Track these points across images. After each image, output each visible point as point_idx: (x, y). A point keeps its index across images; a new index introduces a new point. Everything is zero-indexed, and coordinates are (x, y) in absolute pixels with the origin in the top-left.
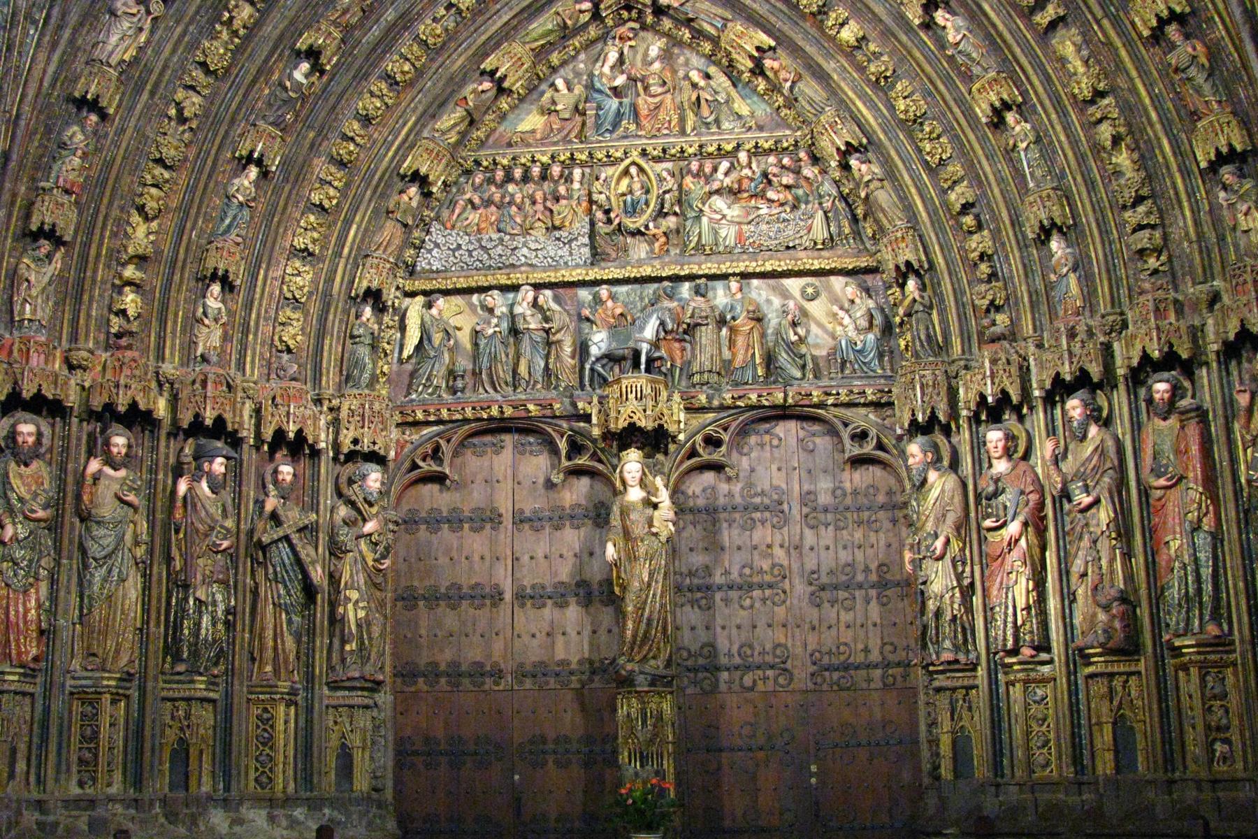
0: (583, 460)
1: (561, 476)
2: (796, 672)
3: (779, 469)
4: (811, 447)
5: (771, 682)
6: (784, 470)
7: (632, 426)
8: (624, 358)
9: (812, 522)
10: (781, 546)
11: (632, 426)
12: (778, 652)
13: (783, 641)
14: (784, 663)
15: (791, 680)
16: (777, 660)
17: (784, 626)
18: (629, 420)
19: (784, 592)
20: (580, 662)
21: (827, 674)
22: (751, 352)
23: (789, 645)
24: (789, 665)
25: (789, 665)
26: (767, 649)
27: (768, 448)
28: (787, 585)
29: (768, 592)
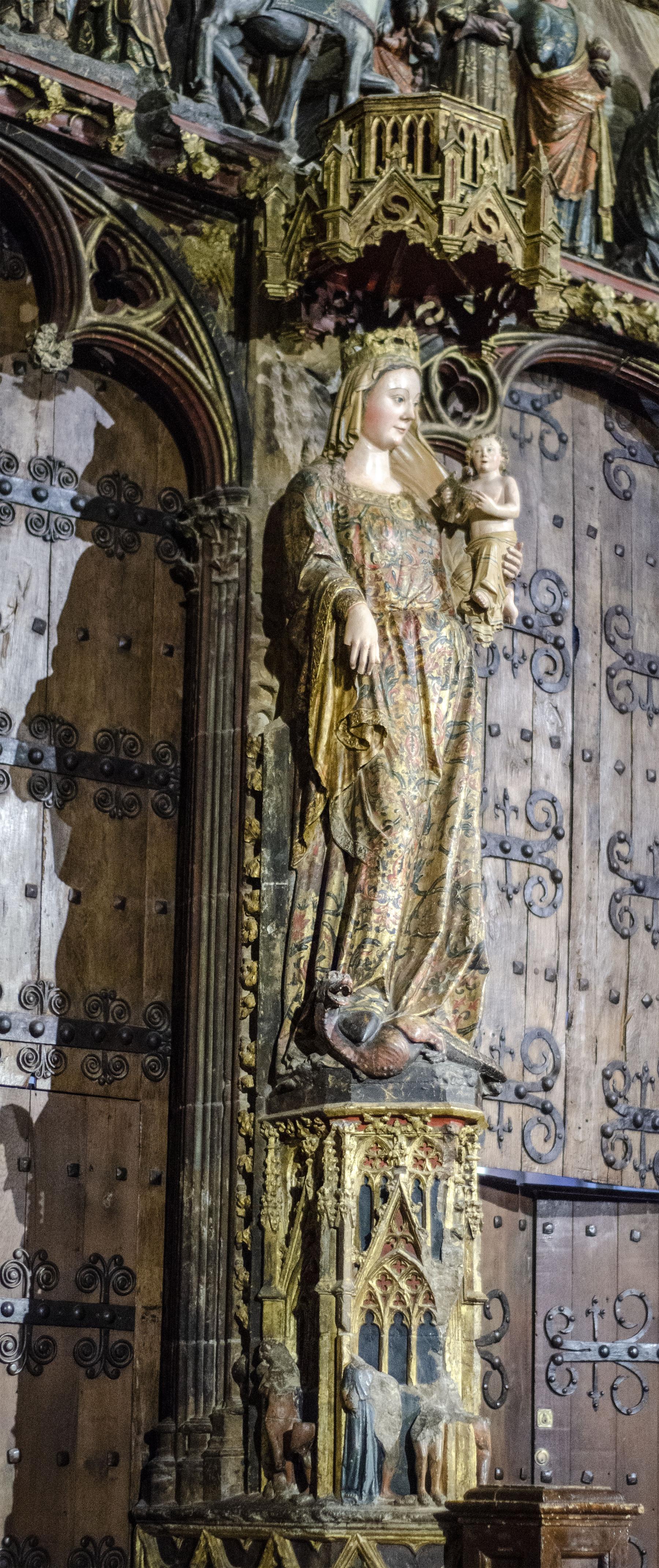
0: (143, 320)
1: (66, 349)
2: (572, 1119)
3: (558, 522)
4: (625, 485)
5: (513, 1140)
6: (568, 527)
7: (487, 252)
8: (292, 51)
9: (621, 695)
10: (555, 743)
11: (487, 252)
12: (534, 1055)
13: (547, 1024)
14: (547, 1088)
15: (559, 1139)
16: (531, 1078)
17: (553, 979)
18: (479, 235)
19: (556, 880)
20: (32, 996)
21: (634, 1137)
22: (593, 167)
23: (560, 1037)
24: (556, 1098)
25: (556, 1098)
26: (510, 1042)
27: (534, 450)
28: (560, 857)
29: (517, 871)
